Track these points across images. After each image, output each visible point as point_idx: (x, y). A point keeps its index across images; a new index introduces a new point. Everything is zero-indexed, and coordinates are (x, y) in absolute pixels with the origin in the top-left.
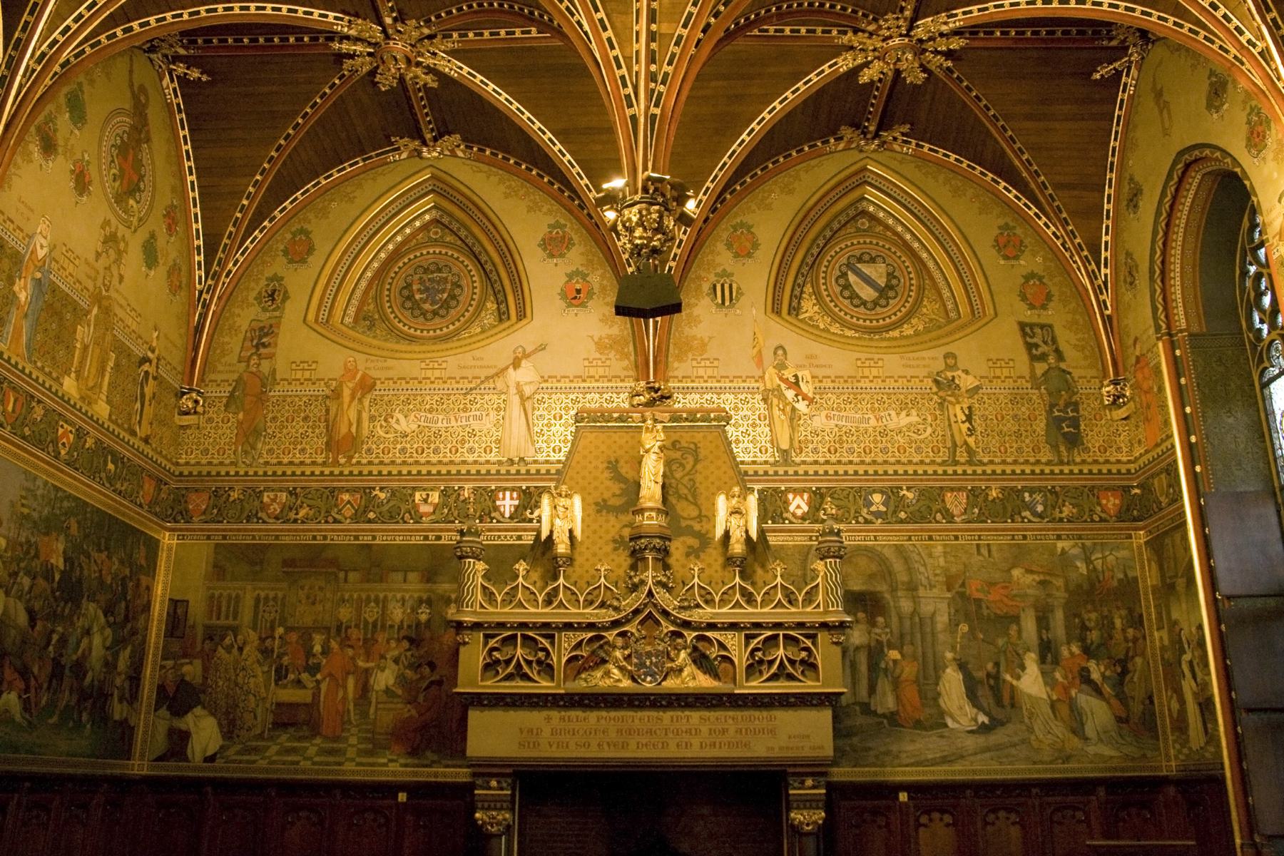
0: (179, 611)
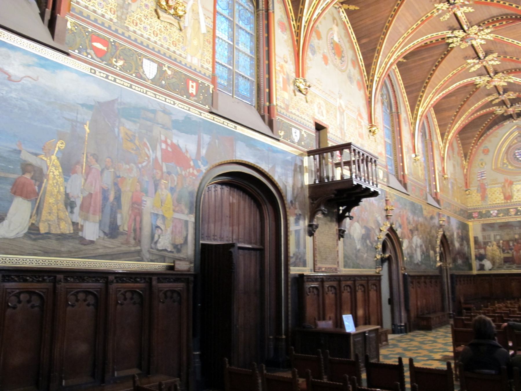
0: (476, 239)
